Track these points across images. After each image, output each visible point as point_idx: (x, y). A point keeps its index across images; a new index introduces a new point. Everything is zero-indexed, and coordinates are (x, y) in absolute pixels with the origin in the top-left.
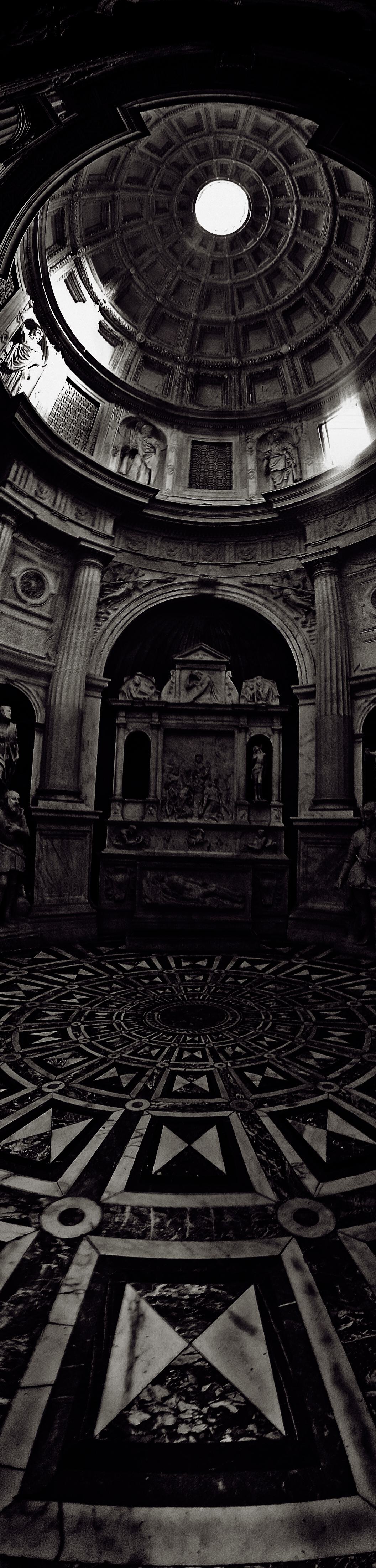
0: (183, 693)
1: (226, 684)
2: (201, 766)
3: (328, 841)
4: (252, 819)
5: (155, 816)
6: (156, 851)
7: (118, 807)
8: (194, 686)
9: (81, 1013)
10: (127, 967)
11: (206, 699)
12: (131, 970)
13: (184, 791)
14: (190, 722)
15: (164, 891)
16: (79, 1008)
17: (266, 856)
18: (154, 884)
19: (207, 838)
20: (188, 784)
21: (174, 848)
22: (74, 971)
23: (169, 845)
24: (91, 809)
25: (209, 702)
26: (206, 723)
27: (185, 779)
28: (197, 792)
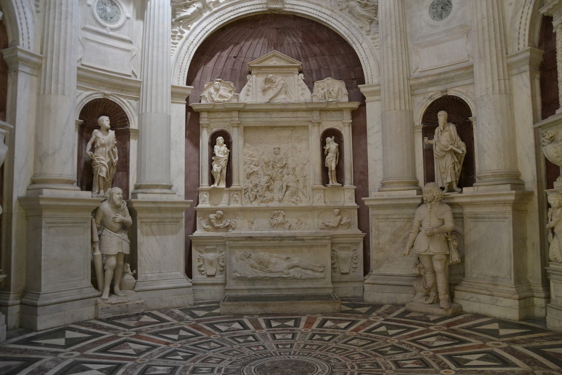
0: (260, 94)
1: (299, 85)
2: (279, 157)
3: (395, 216)
4: (327, 200)
5: (240, 202)
6: (242, 232)
7: (205, 196)
8: (270, 88)
9: (185, 368)
10: (223, 328)
11: (281, 99)
12: (226, 331)
13: (265, 179)
15: (252, 266)
16: (184, 364)
17: (340, 231)
18: (242, 260)
19: (287, 219)
20: (268, 173)
21: (257, 229)
22: (176, 331)
23: (254, 226)
24: (182, 199)
25: (283, 101)
26: (282, 119)
27: (265, 169)
28: (277, 180)
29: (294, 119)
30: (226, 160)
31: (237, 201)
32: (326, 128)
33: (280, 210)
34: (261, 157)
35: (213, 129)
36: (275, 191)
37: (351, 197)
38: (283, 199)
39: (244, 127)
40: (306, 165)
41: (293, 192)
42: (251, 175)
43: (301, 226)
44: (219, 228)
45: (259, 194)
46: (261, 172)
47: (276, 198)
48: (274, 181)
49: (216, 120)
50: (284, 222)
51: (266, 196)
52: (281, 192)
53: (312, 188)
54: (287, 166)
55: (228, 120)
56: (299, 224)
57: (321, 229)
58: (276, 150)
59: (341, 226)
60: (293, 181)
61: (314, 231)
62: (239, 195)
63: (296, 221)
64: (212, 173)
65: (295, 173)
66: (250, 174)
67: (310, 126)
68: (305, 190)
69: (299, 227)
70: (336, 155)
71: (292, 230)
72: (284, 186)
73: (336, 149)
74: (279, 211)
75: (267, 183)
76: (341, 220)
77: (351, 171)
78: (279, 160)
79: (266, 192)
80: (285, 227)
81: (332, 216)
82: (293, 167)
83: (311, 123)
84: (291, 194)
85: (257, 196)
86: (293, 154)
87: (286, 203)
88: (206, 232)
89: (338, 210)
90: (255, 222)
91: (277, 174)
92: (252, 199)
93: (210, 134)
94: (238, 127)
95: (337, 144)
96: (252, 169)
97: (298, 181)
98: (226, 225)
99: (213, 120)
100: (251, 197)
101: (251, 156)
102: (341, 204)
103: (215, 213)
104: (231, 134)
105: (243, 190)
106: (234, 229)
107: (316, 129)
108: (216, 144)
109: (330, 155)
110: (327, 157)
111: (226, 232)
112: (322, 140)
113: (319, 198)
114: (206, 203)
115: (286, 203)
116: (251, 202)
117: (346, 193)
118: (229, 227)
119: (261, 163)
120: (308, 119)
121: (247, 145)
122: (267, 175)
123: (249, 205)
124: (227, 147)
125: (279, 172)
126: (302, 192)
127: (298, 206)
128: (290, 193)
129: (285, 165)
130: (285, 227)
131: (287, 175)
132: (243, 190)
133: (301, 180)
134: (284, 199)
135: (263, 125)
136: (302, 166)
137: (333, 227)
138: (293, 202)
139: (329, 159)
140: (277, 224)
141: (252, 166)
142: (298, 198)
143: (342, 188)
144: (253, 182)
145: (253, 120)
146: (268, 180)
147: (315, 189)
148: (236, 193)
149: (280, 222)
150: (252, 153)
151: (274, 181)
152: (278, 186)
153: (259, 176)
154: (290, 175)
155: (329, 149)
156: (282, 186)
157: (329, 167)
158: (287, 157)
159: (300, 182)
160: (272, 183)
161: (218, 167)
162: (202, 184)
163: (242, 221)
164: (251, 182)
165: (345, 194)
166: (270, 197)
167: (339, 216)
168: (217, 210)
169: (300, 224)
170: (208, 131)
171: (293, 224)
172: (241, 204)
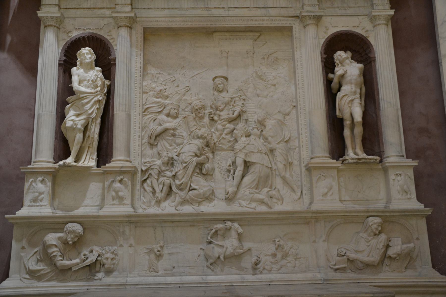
2: (225, 96)
7: (40, 187)
14: (199, 12)
19: (247, 245)
20: (200, 133)
21: (170, 272)
23: (162, 265)
27: (192, 123)
29: (259, 12)
30: (99, 101)
31: (121, 199)
32: (332, 31)
33: (231, 220)
34: (185, 97)
35: (70, 32)
36: (218, 174)
37: (405, 187)
38: (236, 193)
39: (144, 28)
40: (288, 114)
41: (260, 177)
42: (158, 139)
43: (284, 262)
44: (70, 269)
45: (178, 182)
46: (182, 132)
47: (220, 193)
48: (213, 153)
49: (79, 12)
50: (241, 251)
51: (194, 186)
52: (231, 178)
53: (305, 166)
54: (244, 117)
55: (108, 12)
56: (279, 256)
57: (336, 270)
58: (218, 81)
59: (387, 261)
60: (260, 152)
61: (319, 276)
62: (126, 186)
63: (272, 248)
64: (63, 129)
65: (264, 133)
66: (156, 137)
67: (297, 26)
68: (288, 173)
69: (278, 267)
70: (361, 89)
71: (261, 273)
72: (239, 161)
73: (359, 75)
74: (229, 224)
75: (196, 155)
76: (388, 247)
77: (399, 127)
78: (227, 104)
79: (194, 178)
80: (243, 265)
81: (365, 235)
82: (260, 119)
83: (298, 20)
84: (255, 183)
85: (174, 188)
86: (258, 92)
87: (244, 203)
88: (36, 284)
89: (378, 220)
90: (165, 252)
91: (221, 134)
92: (159, 195)
93: (63, 43)
94: (131, 28)
95: (361, 66)
96: (161, 125)
97: (272, 151)
98: (88, 262)
99: (72, 13)
100: (158, 190)
101: (160, 94)
102: (380, 205)
103: (61, 230)
104: (113, 44)
105: (139, 174)
106: (109, 272)
107: (311, 30)
108: (76, 65)
109: (346, 89)
110: (339, 95)
111: (88, 280)
112: (325, 56)
113: (326, 190)
114: (41, 203)
115: (244, 203)
116: (158, 202)
117: (392, 177)
118: (98, 266)
119: (184, 110)
120: (292, 12)
121: (152, 70)
122: (198, 138)
123: (153, 210)
124: (103, 72)
125: (225, 132)
126: (284, 179)
127: (272, 210)
128: (254, 180)
129: (239, 115)
130: (243, 265)
131: (247, 136)
132: (139, 174)
133: (280, 148)
134: (239, 196)
135: (189, 25)
136: (280, 117)
137: (368, 265)
138: (262, 202)
139: (345, 98)
140: (222, 258)
141: (162, 117)
142: (273, 192)
143: (380, 166)
144: (165, 154)
145: (166, 12)
146: (199, 149)
147: (315, 168)
148: (119, 178)
149: (230, 251)
150: (162, 88)
151: (213, 153)
152: (225, 165)
153: (179, 141)
154: (252, 137)
155: (342, 76)
156: (234, 163)
157: (347, 116)
158: (243, 97)
159: (277, 153)
160: (211, 156)
161: (78, 115)
162: (35, 158)
163: (131, 251)
164: (159, 154)
165: (391, 182)
166: (205, 189)
167: (383, 237)
168: (68, 223)
169: (283, 258)
170: (58, 36)
171: (263, 258)
172: (133, 207)
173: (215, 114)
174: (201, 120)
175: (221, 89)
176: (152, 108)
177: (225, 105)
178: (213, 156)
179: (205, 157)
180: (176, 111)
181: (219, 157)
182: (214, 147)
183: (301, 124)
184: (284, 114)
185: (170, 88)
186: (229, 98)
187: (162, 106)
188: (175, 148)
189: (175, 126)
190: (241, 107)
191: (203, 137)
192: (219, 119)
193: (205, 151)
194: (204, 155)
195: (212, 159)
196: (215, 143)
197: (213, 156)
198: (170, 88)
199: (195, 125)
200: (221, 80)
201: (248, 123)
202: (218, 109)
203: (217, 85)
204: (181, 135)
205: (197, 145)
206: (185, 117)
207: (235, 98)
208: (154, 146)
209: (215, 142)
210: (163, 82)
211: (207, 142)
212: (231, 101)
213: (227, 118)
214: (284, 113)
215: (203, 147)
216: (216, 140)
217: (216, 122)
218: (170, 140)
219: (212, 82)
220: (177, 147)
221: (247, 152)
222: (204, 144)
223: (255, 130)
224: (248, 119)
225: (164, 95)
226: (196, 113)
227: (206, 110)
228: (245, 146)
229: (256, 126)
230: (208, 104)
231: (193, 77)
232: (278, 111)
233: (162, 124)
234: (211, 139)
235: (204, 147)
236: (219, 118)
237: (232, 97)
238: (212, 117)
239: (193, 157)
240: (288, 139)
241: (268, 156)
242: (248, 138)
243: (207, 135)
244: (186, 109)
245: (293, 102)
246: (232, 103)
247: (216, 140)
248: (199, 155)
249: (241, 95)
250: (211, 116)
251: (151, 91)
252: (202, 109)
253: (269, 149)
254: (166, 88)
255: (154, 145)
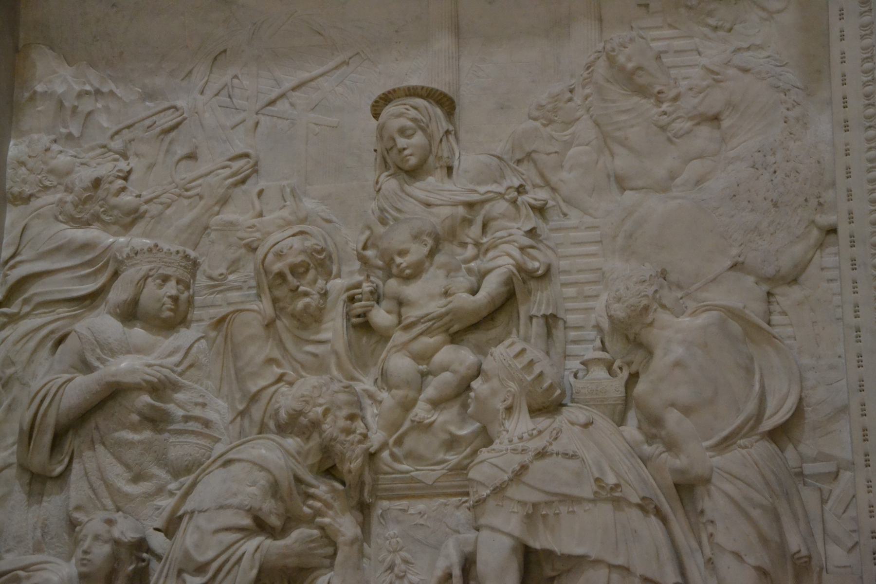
34: (229, 215)
42: (70, 443)
48: (364, 509)
65: (641, 387)
75: (261, 526)
82: (619, 311)
86: (623, 162)
91: (407, 406)
96: (86, 367)
119: (217, 284)
122: (283, 429)
125: (430, 391)
131: (535, 411)
144: (94, 524)
146: (274, 490)
150: (106, 168)
151: (364, 509)
154: (574, 413)
173: (377, 296)
174: (305, 335)
175: (413, 161)
176: (47, 280)
177: (430, 242)
178: (365, 526)
179: (316, 532)
180: (171, 288)
181: (393, 530)
182: (368, 478)
183: (858, 330)
184: (768, 279)
185: (151, 167)
186: (455, 204)
187: (106, 265)
188: (160, 491)
189: (167, 372)
190: (522, 249)
191: (303, 420)
192: (400, 323)
193: (310, 502)
194: (309, 521)
195: (353, 542)
196: (372, 456)
197: (365, 526)
198: (151, 167)
199: (271, 361)
200: (416, 108)
201: (559, 333)
202: (395, 270)
203: (394, 140)
204: (196, 419)
205: (262, 468)
206: (222, 320)
207: (487, 207)
208: (49, 485)
209: (372, 450)
210: (112, 137)
211: (326, 450)
212: (468, 222)
213: (441, 317)
214: (770, 270)
215: (298, 480)
216: (376, 438)
217: (384, 337)
218: (131, 444)
219: (374, 123)
220: (172, 486)
221: (535, 497)
222: (310, 462)
223: (599, 373)
224: (561, 314)
225: (114, 207)
226: (278, 293)
227: (339, 276)
228: (524, 468)
229: (604, 349)
230: (347, 243)
231: (272, 103)
232: (729, 263)
233: (96, 364)
234: (348, 432)
235: (309, 477)
236: (400, 315)
237: (475, 197)
238: (359, 311)
239: (238, 535)
240: (787, 422)
241: (664, 520)
242: (543, 422)
243: (326, 412)
244: (231, 277)
245: (820, 204)
246: (475, 231)
247: (376, 438)
248: (274, 521)
249: (521, 186)
250: (358, 307)
251: (46, 188)
252: (312, 274)
253: (669, 480)
254: (129, 172)
255: (51, 478)
